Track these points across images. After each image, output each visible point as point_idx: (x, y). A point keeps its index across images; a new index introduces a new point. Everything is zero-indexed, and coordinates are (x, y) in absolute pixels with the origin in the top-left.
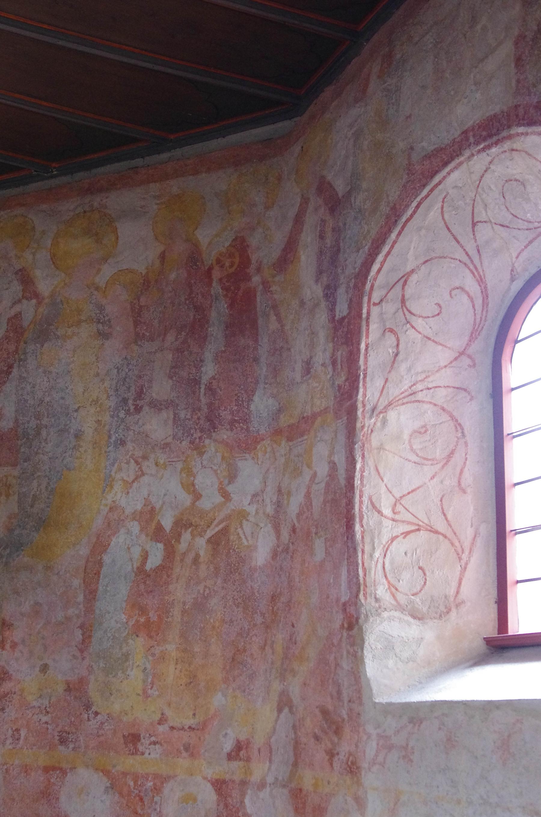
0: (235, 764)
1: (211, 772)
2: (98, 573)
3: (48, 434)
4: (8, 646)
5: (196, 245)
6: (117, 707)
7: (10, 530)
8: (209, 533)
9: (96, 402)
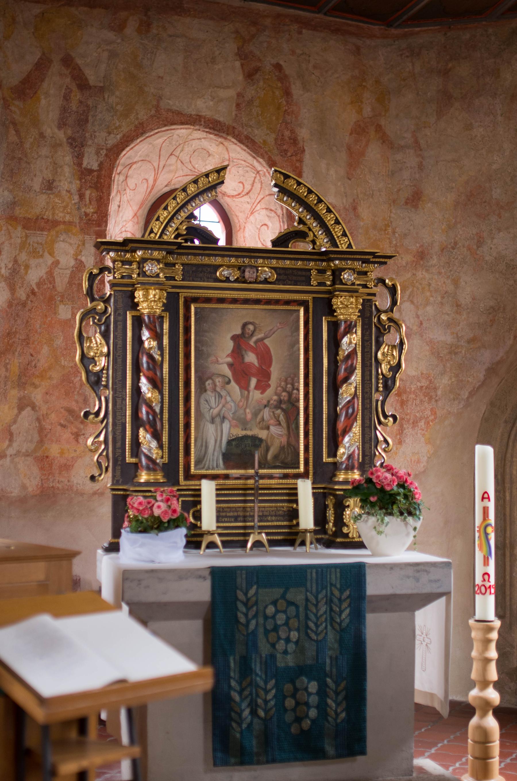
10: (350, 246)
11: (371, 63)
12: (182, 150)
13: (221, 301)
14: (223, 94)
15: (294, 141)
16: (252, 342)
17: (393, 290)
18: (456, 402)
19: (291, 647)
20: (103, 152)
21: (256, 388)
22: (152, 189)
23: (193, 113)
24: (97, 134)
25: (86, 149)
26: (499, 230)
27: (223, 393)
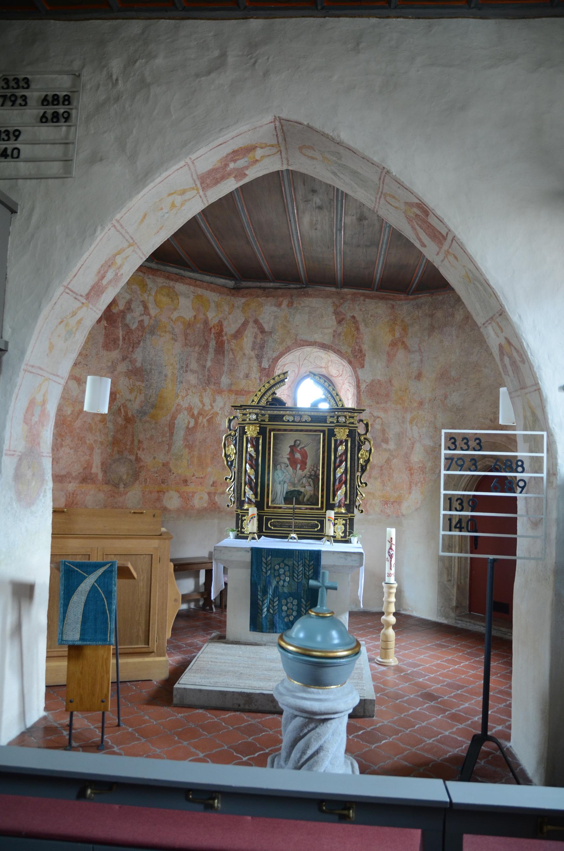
0: (213, 488)
1: (206, 490)
2: (174, 427)
3: (155, 373)
4: (141, 450)
5: (207, 318)
6: (180, 471)
7: (142, 407)
8: (207, 418)
9: (172, 364)
10: (343, 406)
11: (400, 312)
12: (310, 357)
13: (285, 430)
14: (326, 331)
15: (361, 351)
16: (298, 449)
17: (367, 425)
18: (434, 475)
19: (286, 584)
20: (271, 360)
21: (300, 469)
22: (298, 375)
23: (313, 340)
24: (268, 352)
25: (264, 359)
26: (454, 391)
27: (285, 471)
